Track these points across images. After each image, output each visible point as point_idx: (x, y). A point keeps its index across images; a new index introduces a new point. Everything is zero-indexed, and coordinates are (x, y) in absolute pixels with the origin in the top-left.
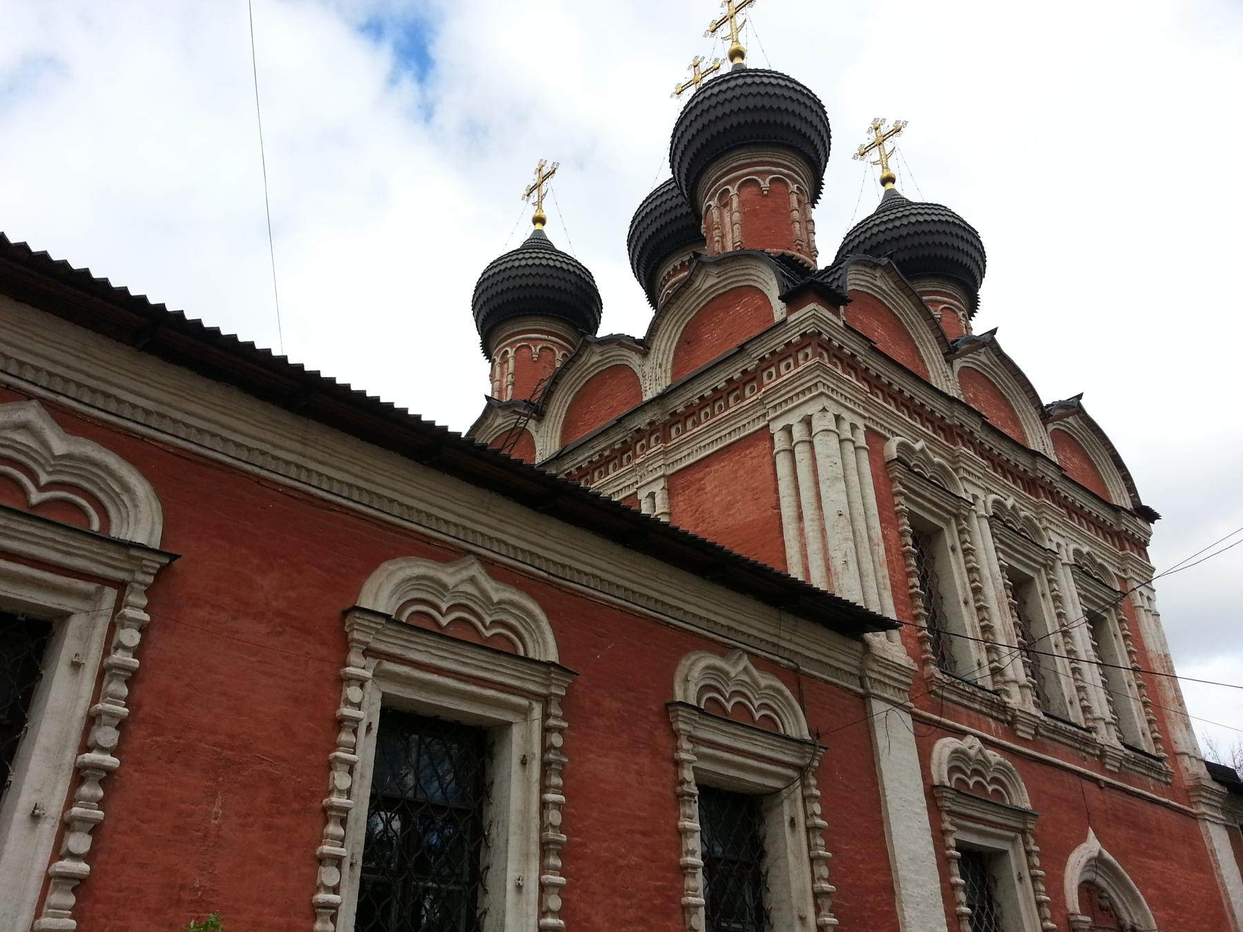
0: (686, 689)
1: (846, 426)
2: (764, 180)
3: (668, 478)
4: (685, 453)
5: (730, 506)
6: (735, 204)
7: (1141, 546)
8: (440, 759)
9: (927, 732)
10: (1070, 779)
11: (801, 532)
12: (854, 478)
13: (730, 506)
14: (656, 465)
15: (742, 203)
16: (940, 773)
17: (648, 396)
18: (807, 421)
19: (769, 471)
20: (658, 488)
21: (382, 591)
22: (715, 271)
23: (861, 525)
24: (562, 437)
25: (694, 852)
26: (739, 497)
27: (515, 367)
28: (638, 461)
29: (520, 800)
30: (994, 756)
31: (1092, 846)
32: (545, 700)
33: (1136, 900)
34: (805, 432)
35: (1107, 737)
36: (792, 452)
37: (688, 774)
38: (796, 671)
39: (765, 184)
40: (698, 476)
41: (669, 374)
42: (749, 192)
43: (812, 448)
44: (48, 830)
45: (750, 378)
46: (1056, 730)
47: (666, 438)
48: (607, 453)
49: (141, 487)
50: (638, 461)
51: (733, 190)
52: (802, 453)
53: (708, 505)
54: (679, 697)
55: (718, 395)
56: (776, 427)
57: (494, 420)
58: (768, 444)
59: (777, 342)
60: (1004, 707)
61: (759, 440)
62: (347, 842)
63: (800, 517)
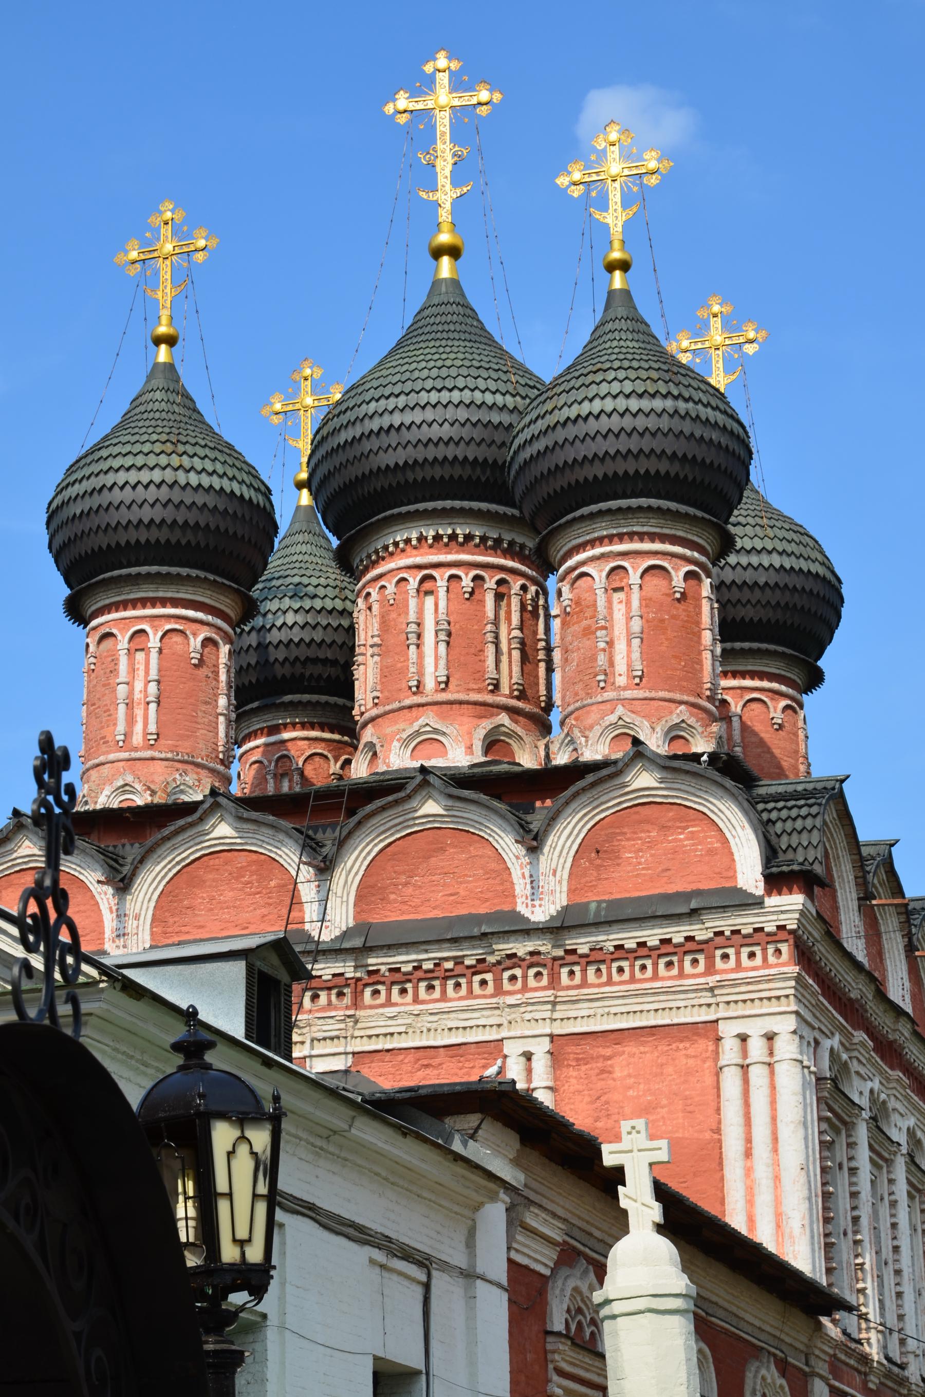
2: (677, 570)
4: (585, 1013)
11: (748, 1172)
14: (538, 1016)
15: (646, 602)
18: (770, 1037)
19: (709, 1080)
20: (540, 1048)
26: (664, 1102)
27: (160, 670)
28: (511, 1000)
34: (766, 1051)
36: (745, 1068)
40: (608, 1052)
41: (565, 889)
42: (654, 581)
43: (772, 1073)
48: (449, 965)
50: (511, 1000)
51: (634, 577)
52: (758, 1075)
53: (616, 1096)
56: (728, 1030)
57: (214, 826)
58: (711, 1047)
59: (746, 921)
61: (698, 1034)
63: (748, 1153)
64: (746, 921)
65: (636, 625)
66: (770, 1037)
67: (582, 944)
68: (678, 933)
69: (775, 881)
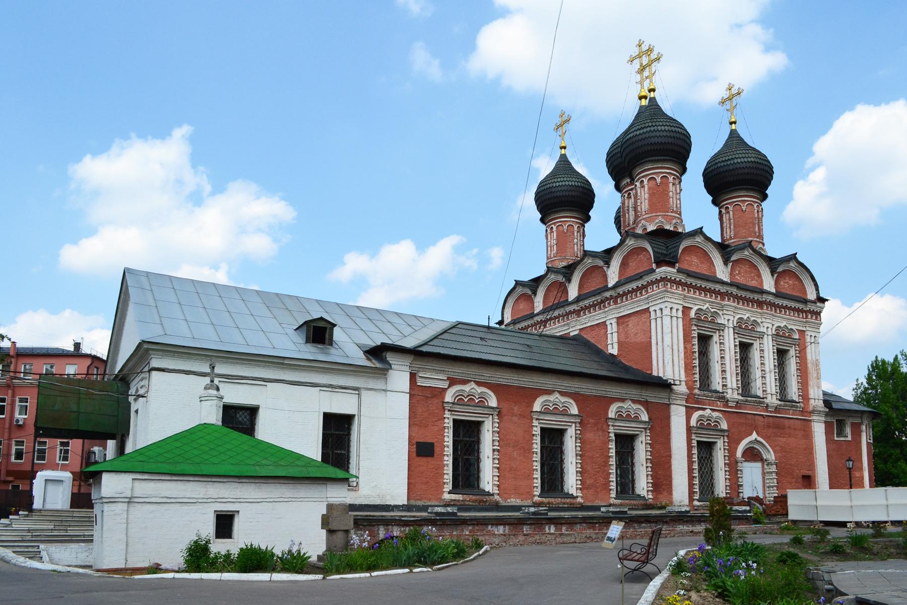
0: (611, 414)
1: (674, 311)
3: (618, 318)
5: (636, 334)
6: (646, 187)
7: (818, 314)
8: (553, 439)
9: (689, 412)
10: (750, 416)
12: (675, 330)
13: (636, 334)
15: (649, 189)
16: (693, 423)
17: (610, 285)
18: (661, 309)
20: (614, 321)
21: (537, 406)
22: (633, 239)
23: (675, 348)
24: (579, 288)
25: (613, 453)
29: (570, 445)
30: (715, 414)
31: (754, 436)
32: (575, 423)
33: (769, 451)
35: (773, 400)
37: (612, 435)
38: (647, 401)
39: (659, 180)
42: (652, 182)
44: (491, 459)
45: (644, 287)
46: (747, 401)
47: (616, 303)
49: (492, 394)
51: (646, 182)
52: (659, 320)
54: (610, 416)
55: (633, 291)
56: (651, 309)
59: (652, 277)
60: (724, 397)
62: (537, 457)
64: (652, 277)
65: (647, 196)
66: (661, 309)
67: (620, 290)
68: (639, 283)
69: (659, 263)
